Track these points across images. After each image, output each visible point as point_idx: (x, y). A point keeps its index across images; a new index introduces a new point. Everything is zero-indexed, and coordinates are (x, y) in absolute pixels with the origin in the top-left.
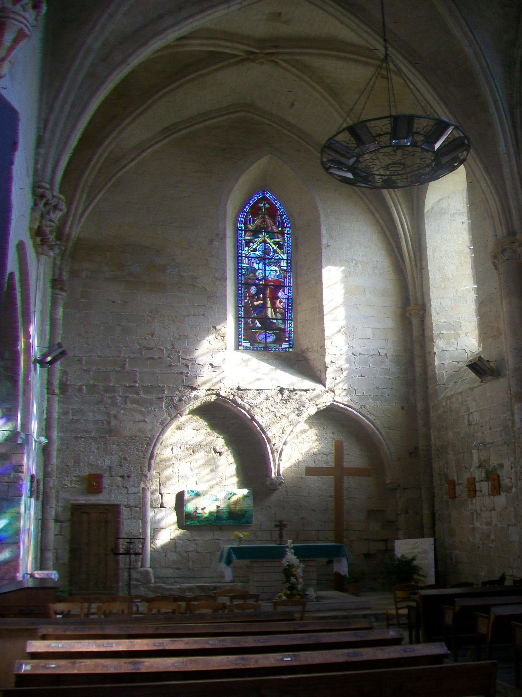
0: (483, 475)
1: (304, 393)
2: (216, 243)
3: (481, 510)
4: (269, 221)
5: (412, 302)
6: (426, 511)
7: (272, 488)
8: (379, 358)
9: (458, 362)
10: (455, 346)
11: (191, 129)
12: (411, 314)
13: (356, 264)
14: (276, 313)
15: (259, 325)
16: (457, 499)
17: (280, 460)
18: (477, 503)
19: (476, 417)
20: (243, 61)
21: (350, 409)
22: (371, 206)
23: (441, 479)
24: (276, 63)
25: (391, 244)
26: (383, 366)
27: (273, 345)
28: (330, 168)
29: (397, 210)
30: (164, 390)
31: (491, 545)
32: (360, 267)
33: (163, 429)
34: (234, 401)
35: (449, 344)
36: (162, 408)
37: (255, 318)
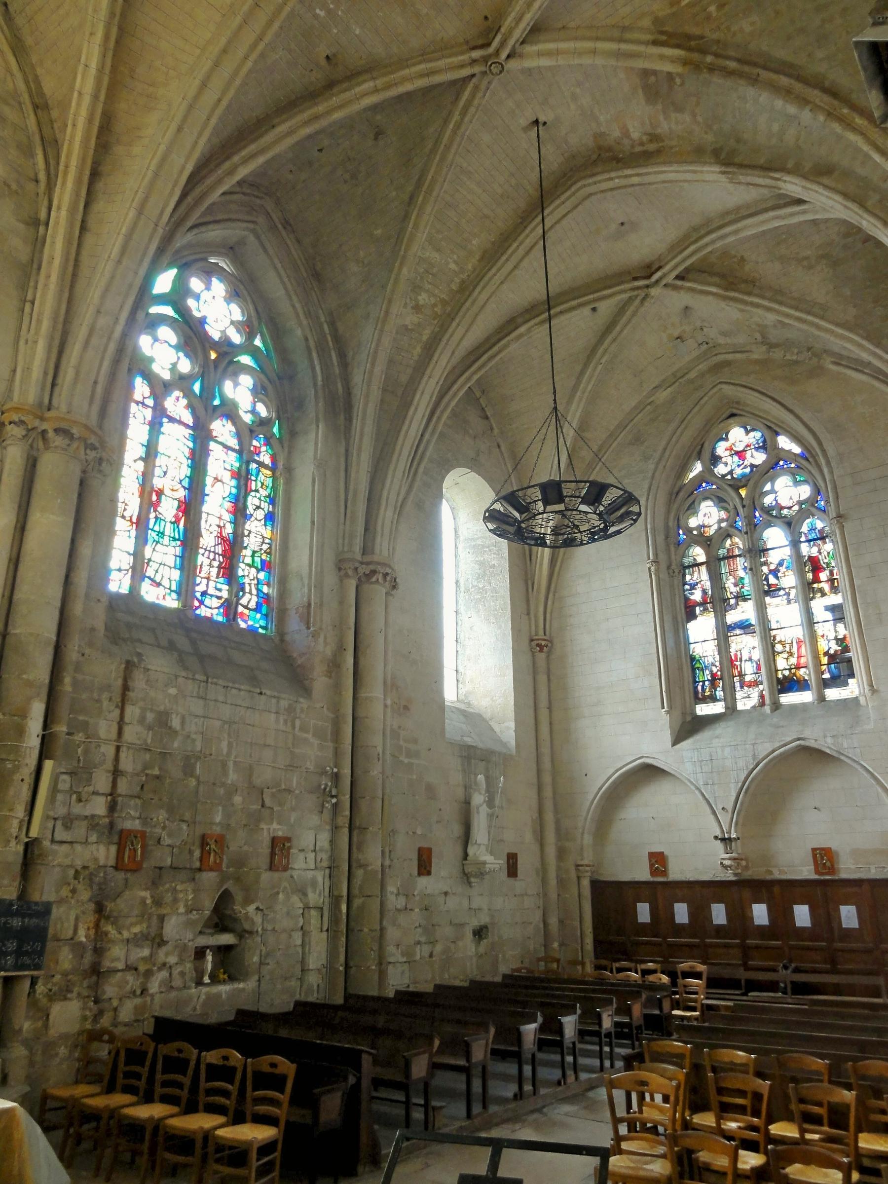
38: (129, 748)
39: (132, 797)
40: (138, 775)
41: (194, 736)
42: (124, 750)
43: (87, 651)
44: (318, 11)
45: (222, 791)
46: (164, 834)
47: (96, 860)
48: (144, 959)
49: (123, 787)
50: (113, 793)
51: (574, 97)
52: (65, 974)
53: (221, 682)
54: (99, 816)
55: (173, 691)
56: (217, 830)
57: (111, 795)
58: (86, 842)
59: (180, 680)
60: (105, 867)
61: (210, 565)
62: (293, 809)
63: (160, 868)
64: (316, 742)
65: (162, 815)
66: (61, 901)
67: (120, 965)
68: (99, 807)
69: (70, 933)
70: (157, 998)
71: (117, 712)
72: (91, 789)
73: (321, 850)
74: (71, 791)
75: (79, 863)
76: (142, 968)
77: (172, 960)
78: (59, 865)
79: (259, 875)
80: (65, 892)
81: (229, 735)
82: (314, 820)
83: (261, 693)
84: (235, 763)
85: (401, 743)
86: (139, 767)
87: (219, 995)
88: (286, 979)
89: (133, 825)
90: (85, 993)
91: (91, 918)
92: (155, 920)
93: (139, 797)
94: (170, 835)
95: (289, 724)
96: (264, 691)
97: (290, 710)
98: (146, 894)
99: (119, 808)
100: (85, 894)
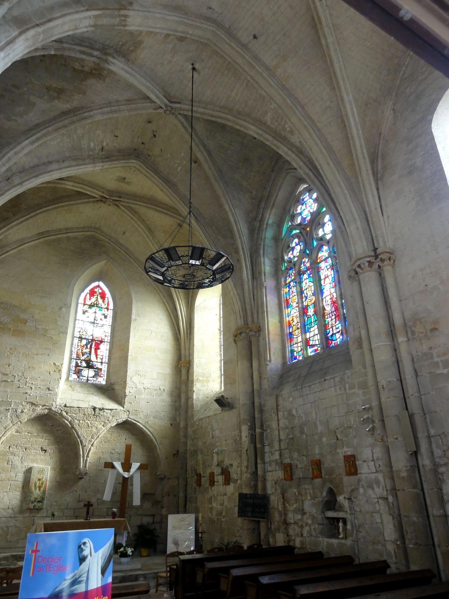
0: (220, 471)
1: (110, 411)
2: (64, 309)
3: (217, 495)
4: (100, 301)
5: (183, 359)
6: (181, 495)
7: (80, 476)
8: (159, 392)
9: (207, 397)
10: (207, 388)
11: (58, 236)
12: (181, 366)
13: (151, 332)
14: (97, 358)
15: (85, 365)
17: (88, 456)
19: (217, 432)
20: (98, 201)
21: (138, 424)
22: (164, 299)
24: (119, 206)
25: (173, 324)
26: (161, 397)
27: (92, 379)
28: (150, 271)
29: (179, 303)
30: (11, 404)
31: (223, 520)
32: (153, 334)
33: (5, 432)
34: (61, 414)
35: (203, 386)
36: (7, 417)
37: (83, 360)
41: (301, 415)
42: (280, 431)
44: (179, 170)
45: (316, 437)
47: (279, 477)
48: (299, 519)
50: (280, 450)
51: (170, 62)
53: (307, 385)
55: (291, 399)
56: (317, 457)
58: (276, 471)
59: (293, 393)
60: (282, 479)
61: (332, 320)
62: (355, 437)
63: (300, 478)
64: (360, 392)
65: (296, 455)
67: (292, 522)
68: (277, 456)
73: (378, 459)
77: (310, 522)
79: (341, 479)
81: (315, 408)
82: (370, 440)
83: (325, 380)
84: (320, 421)
85: (436, 360)
87: (332, 544)
88: (374, 544)
89: (287, 461)
90: (284, 531)
91: (282, 500)
92: (301, 502)
93: (287, 449)
95: (343, 388)
96: (326, 378)
97: (342, 380)
98: (295, 490)
100: (279, 491)
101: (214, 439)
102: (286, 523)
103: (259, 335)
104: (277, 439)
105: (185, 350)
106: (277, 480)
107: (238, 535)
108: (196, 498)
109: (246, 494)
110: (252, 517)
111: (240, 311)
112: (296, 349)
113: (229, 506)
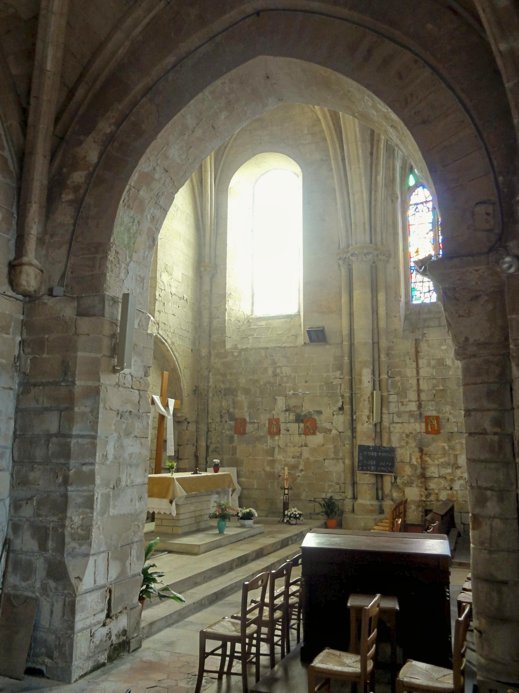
0: (292, 417)
3: (286, 446)
16: (247, 435)
18: (280, 440)
23: (221, 417)
38: (424, 379)
39: (429, 401)
40: (430, 390)
43: (395, 340)
46: (450, 417)
47: (415, 430)
49: (423, 396)
50: (419, 400)
52: (409, 477)
54: (414, 411)
55: (444, 347)
57: (418, 401)
60: (420, 432)
63: (452, 433)
65: (448, 408)
66: (401, 447)
67: (437, 475)
68: (413, 407)
69: (408, 460)
70: (459, 492)
71: (415, 364)
72: (407, 399)
74: (398, 402)
75: (407, 432)
76: (449, 478)
78: (398, 432)
80: (403, 443)
86: (431, 387)
90: (420, 485)
91: (418, 454)
92: (452, 456)
94: (454, 418)
98: (445, 445)
99: (423, 406)
100: (414, 445)
101: (278, 379)
102: (424, 477)
103: (388, 262)
104: (415, 388)
105: (210, 247)
106: (411, 433)
107: (330, 491)
108: (234, 449)
109: (369, 447)
110: (377, 471)
111: (364, 224)
112: (419, 288)
113: (312, 459)
